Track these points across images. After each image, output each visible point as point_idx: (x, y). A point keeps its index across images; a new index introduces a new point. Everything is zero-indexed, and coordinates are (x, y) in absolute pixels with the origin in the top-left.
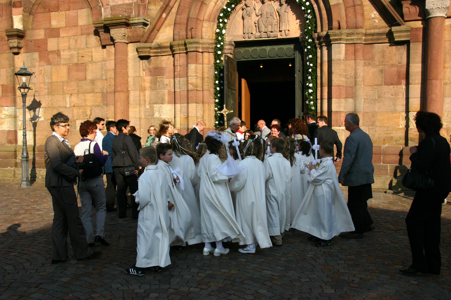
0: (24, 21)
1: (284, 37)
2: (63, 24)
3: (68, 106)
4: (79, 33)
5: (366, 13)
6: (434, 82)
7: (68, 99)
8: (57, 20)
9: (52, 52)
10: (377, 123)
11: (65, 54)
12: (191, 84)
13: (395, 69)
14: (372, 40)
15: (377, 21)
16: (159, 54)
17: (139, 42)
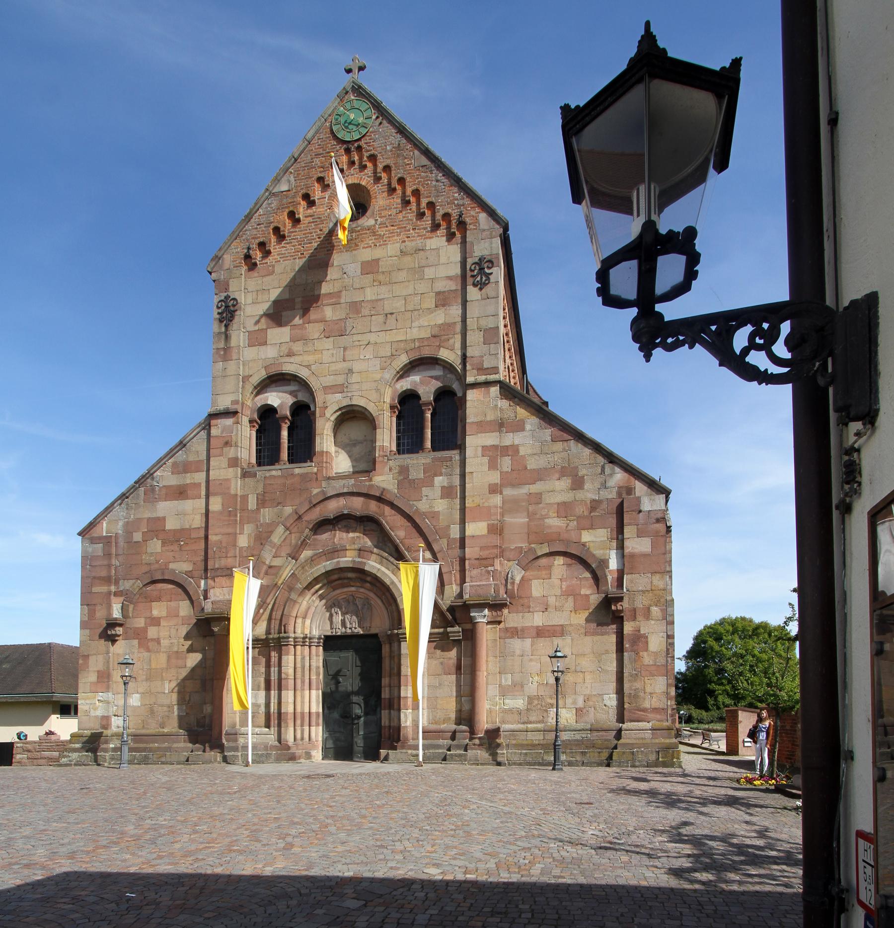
0: (123, 609)
2: (164, 614)
3: (167, 691)
4: (180, 622)
6: (478, 673)
7: (167, 685)
8: (158, 610)
9: (152, 640)
10: (438, 706)
11: (165, 643)
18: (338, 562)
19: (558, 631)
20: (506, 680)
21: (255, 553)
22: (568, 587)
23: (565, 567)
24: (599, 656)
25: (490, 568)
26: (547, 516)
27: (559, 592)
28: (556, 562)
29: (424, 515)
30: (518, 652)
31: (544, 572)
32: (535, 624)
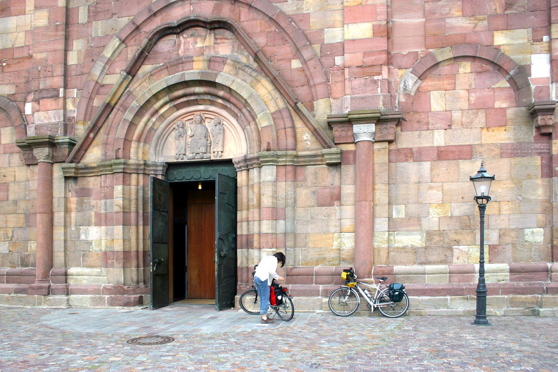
1: (218, 158)
5: (298, 135)
12: (117, 205)
13: (328, 190)
14: (304, 162)
15: (309, 143)
16: (86, 175)
17: (64, 162)
18: (184, 74)
19: (466, 153)
20: (398, 212)
21: (85, 70)
22: (478, 98)
23: (473, 76)
24: (518, 183)
25: (376, 78)
26: (448, 15)
27: (465, 106)
28: (461, 70)
29: (290, 19)
30: (414, 178)
31: (446, 82)
32: (436, 144)
